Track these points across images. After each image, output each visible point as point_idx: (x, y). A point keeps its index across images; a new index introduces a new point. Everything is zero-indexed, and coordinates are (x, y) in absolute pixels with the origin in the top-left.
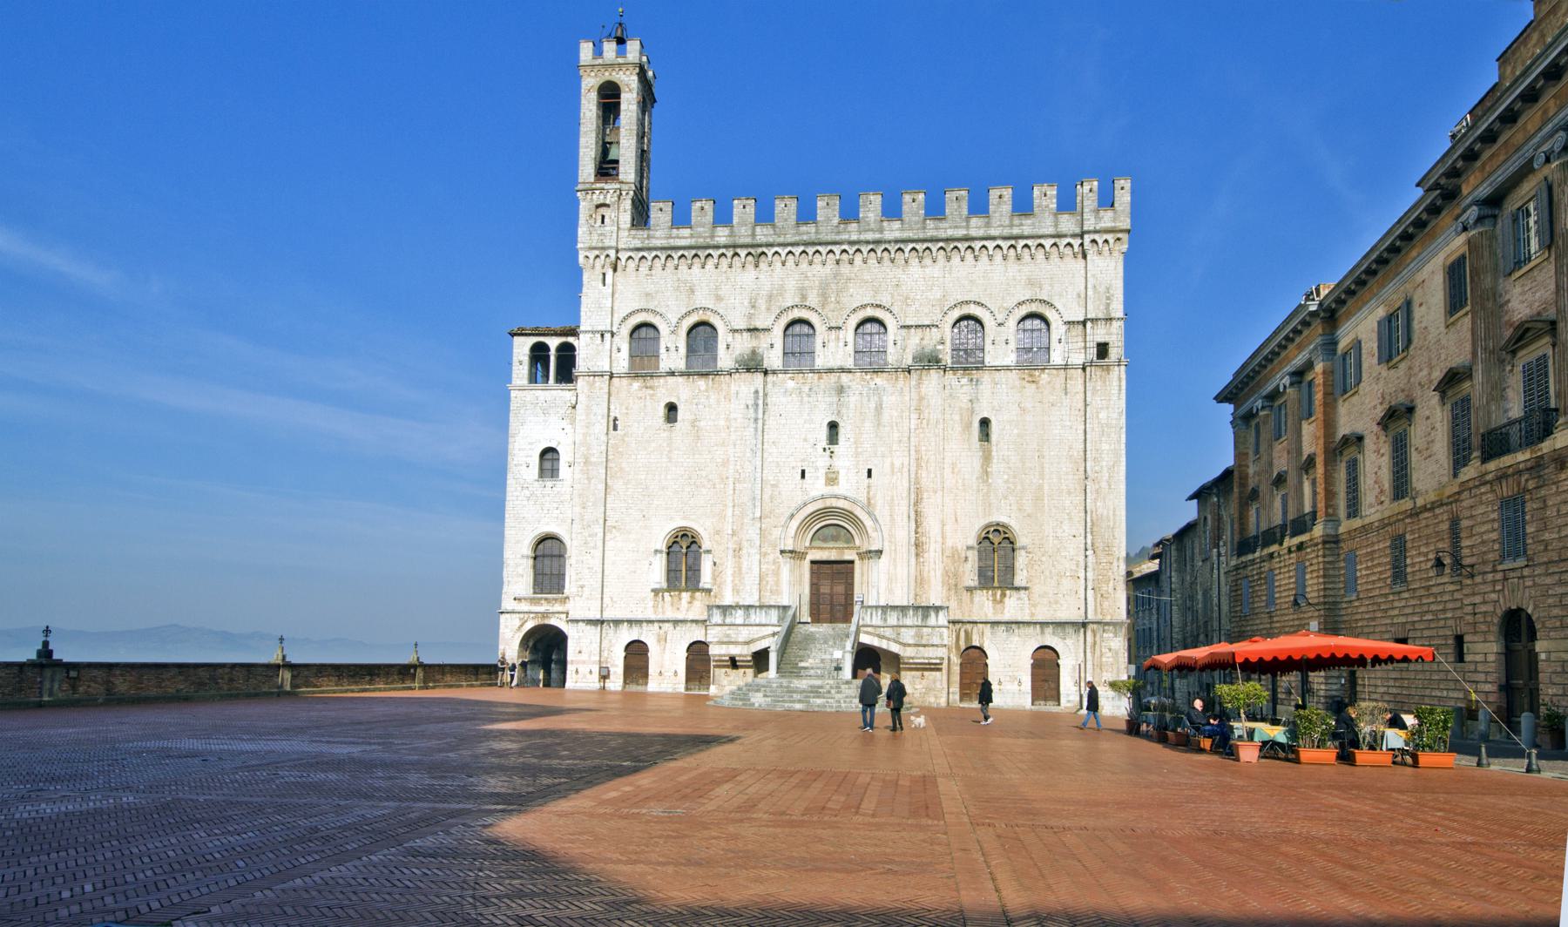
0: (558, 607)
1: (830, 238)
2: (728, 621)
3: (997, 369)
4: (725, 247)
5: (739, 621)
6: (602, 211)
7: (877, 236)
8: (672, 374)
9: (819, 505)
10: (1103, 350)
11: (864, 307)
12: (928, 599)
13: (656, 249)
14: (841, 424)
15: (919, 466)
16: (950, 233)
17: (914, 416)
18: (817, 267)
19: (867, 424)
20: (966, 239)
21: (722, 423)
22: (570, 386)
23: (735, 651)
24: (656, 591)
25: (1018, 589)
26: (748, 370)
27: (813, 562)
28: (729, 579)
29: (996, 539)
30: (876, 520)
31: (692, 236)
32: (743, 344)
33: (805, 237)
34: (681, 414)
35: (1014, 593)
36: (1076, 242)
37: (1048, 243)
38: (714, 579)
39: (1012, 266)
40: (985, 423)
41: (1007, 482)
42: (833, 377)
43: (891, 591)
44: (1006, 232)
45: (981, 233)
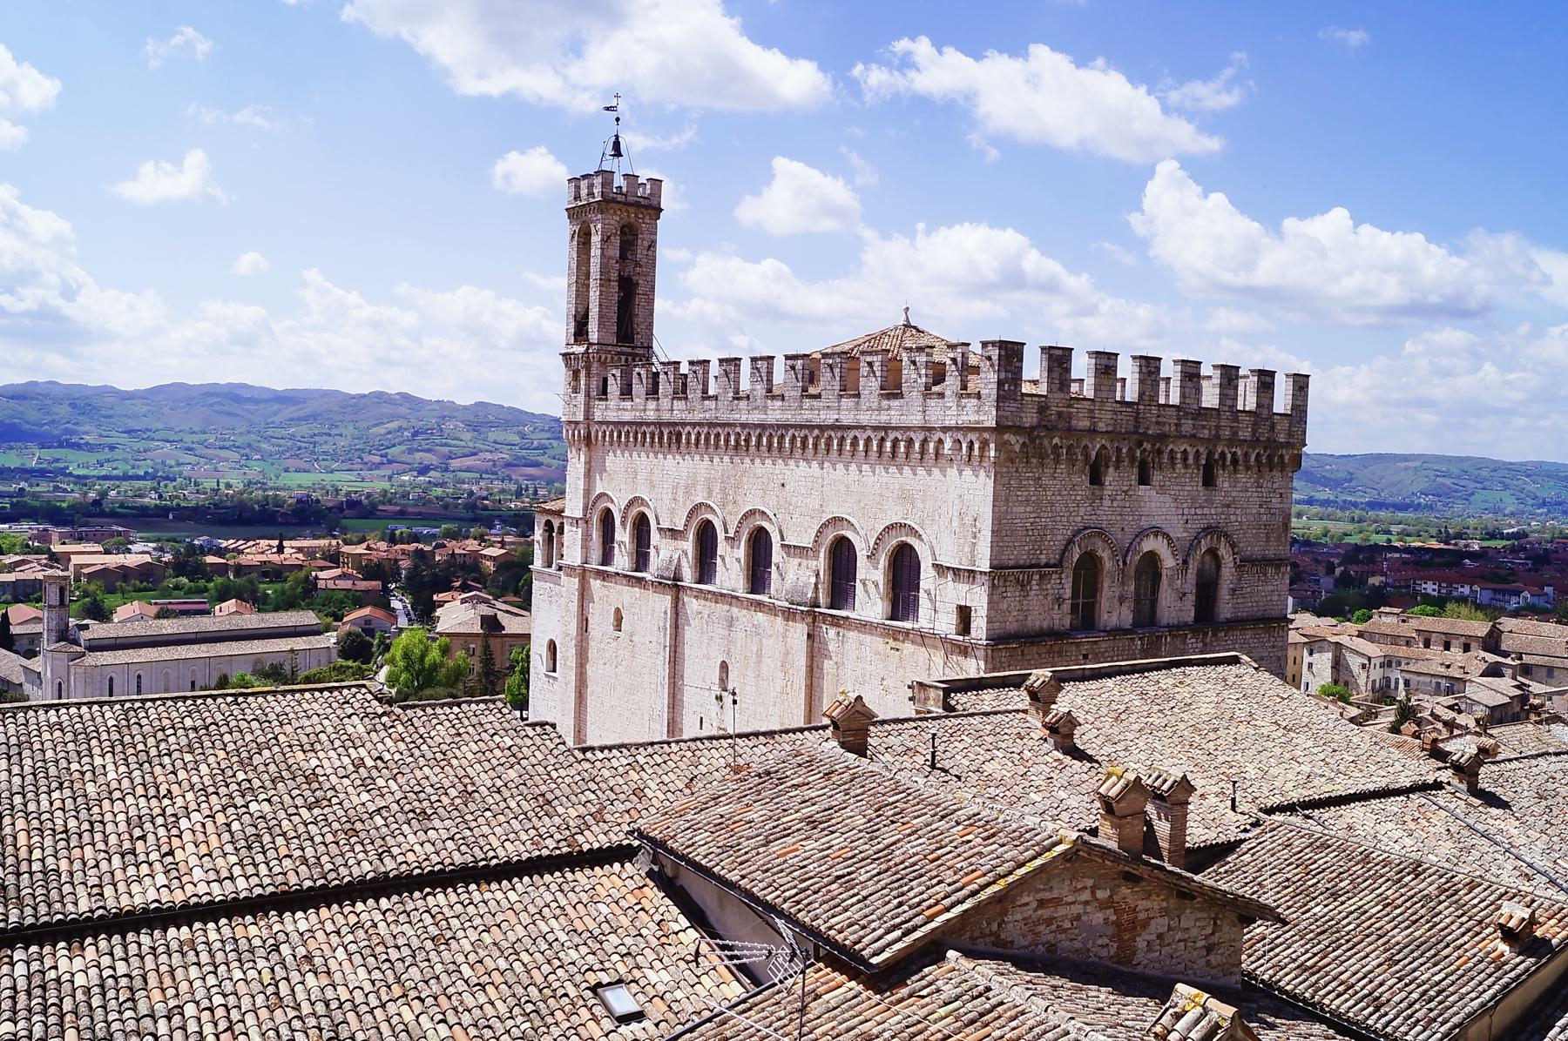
10: (964, 614)
11: (752, 512)
20: (836, 427)
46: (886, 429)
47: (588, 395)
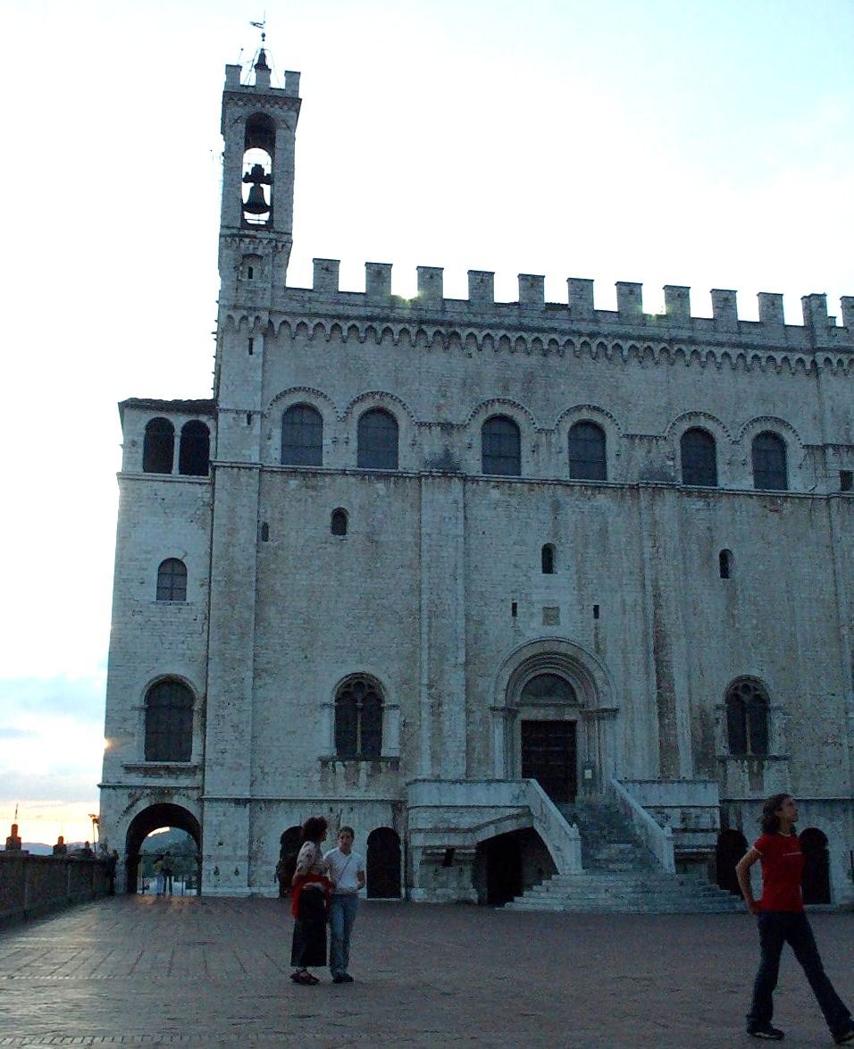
0: (184, 781)
1: (535, 323)
2: (446, 801)
3: (734, 494)
4: (410, 321)
5: (460, 802)
6: (250, 263)
7: (592, 327)
8: (344, 473)
9: (537, 649)
11: (579, 408)
12: (678, 771)
13: (317, 315)
14: (559, 548)
15: (657, 606)
16: (674, 333)
17: (648, 543)
18: (520, 358)
19: (591, 551)
21: (409, 539)
22: (205, 479)
23: (455, 841)
24: (324, 762)
25: (776, 759)
26: (445, 474)
27: (525, 724)
28: (425, 746)
29: (746, 698)
30: (607, 672)
31: (366, 305)
32: (433, 444)
33: (507, 321)
34: (353, 523)
35: (776, 766)
36: (808, 359)
37: (779, 356)
38: (403, 743)
39: (743, 380)
40: (725, 556)
41: (756, 627)
42: (548, 491)
43: (630, 763)
44: (734, 338)
45: (708, 337)
46: (746, 346)
47: (273, 286)
